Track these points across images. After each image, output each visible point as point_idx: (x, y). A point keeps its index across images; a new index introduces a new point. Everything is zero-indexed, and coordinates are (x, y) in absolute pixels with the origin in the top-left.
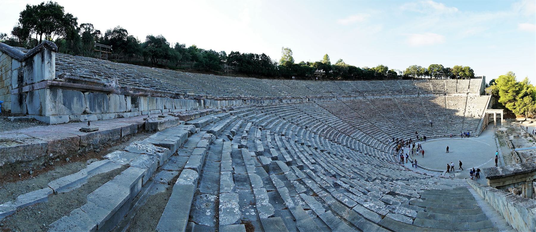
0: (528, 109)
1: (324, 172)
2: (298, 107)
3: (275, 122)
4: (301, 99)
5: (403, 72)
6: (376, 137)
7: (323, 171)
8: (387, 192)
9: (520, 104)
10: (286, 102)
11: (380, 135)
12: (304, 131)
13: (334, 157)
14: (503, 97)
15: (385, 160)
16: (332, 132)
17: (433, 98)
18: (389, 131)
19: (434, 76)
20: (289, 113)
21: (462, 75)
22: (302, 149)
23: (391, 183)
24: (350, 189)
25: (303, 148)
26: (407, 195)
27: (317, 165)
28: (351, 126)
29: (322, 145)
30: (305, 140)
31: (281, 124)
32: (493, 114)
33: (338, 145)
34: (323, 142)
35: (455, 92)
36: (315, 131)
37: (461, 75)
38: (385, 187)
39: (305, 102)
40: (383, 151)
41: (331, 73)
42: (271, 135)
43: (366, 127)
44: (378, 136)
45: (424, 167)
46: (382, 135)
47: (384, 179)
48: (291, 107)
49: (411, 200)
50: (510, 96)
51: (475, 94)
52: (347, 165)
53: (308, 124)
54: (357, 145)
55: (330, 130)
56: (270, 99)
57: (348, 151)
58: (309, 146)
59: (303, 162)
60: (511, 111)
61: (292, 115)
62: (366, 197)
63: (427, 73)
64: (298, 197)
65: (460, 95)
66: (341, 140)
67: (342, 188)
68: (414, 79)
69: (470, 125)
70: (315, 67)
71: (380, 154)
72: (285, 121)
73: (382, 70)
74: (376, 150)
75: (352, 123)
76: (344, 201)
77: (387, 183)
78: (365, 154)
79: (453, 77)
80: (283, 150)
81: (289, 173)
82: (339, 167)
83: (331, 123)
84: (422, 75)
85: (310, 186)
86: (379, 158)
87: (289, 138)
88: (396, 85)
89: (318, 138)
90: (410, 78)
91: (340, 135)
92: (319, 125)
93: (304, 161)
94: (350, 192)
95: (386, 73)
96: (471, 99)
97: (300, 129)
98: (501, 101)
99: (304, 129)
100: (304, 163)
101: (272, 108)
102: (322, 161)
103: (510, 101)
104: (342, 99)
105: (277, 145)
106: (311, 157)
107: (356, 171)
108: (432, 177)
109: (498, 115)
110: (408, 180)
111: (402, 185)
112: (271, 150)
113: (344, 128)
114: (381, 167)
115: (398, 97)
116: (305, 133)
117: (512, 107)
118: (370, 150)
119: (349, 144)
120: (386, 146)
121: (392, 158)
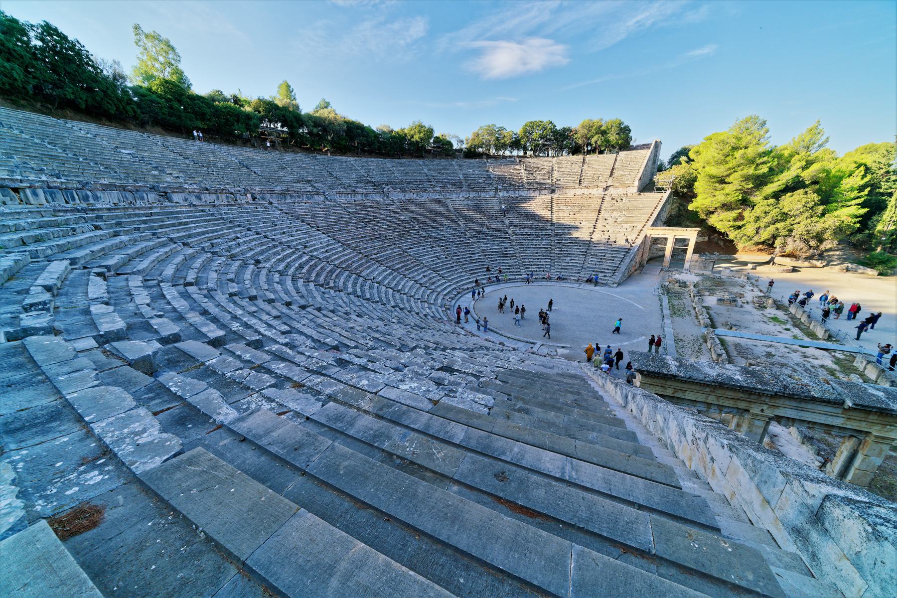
0: (791, 230)
1: (313, 344)
2: (226, 214)
3: (157, 255)
4: (232, 193)
5: (465, 142)
6: (411, 276)
7: (309, 342)
8: (437, 367)
9: (763, 215)
10: (186, 200)
11: (420, 271)
12: (253, 271)
13: (331, 315)
14: (706, 196)
15: (429, 317)
16: (321, 269)
17: (528, 199)
18: (437, 264)
19: (531, 150)
20: (200, 230)
21: (599, 143)
22: (254, 309)
23: (443, 353)
24: (370, 366)
25: (256, 305)
26: (474, 373)
27: (295, 335)
28: (360, 256)
29: (302, 297)
30: (259, 288)
31: (180, 258)
32: (666, 239)
33: (338, 293)
34: (303, 290)
35: (577, 186)
36: (281, 268)
37: (596, 143)
38: (433, 359)
39: (243, 202)
40: (425, 302)
41: (302, 136)
42: (146, 287)
43: (391, 257)
44: (416, 273)
45: (501, 332)
46: (423, 272)
47: (429, 348)
48: (202, 213)
49: (481, 380)
50: (731, 192)
51: (621, 191)
52: (358, 328)
53: (261, 253)
54: (375, 290)
55: (316, 265)
56: (124, 188)
57: (359, 304)
58: (270, 301)
59: (260, 333)
60: (724, 234)
61: (210, 235)
62: (402, 375)
63: (516, 144)
64: (258, 397)
65: (586, 192)
66: (341, 284)
67: (353, 365)
68: (489, 156)
69: (602, 259)
70: (259, 112)
71: (420, 306)
72: (191, 251)
73: (422, 135)
74: (412, 299)
75: (363, 249)
76: (361, 384)
77: (437, 354)
78: (393, 307)
79: (576, 150)
80: (194, 318)
81: (218, 361)
82: (344, 333)
83: (316, 250)
84: (506, 149)
85: (285, 372)
86: (417, 314)
87: (210, 290)
88: (450, 171)
89: (289, 283)
90: (480, 156)
91: (340, 274)
92: (289, 256)
93: (262, 330)
94: (369, 370)
95: (429, 143)
96: (614, 201)
97: (240, 266)
98: (697, 208)
99: (252, 267)
100: (264, 335)
101: (136, 215)
102: (304, 325)
103: (727, 207)
104: (337, 197)
105: (174, 308)
106: (279, 322)
107: (377, 335)
108: (514, 349)
109: (684, 242)
110: (472, 351)
111: (463, 358)
112: (152, 322)
113: (347, 260)
114: (422, 328)
115: (454, 196)
116: (256, 275)
117: (731, 223)
118: (402, 300)
119: (358, 290)
120: (431, 293)
121: (442, 314)
